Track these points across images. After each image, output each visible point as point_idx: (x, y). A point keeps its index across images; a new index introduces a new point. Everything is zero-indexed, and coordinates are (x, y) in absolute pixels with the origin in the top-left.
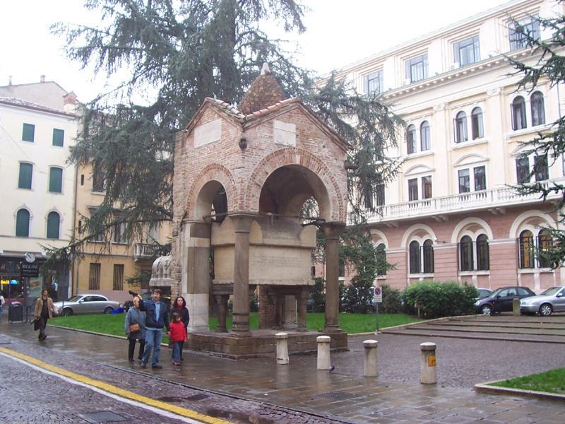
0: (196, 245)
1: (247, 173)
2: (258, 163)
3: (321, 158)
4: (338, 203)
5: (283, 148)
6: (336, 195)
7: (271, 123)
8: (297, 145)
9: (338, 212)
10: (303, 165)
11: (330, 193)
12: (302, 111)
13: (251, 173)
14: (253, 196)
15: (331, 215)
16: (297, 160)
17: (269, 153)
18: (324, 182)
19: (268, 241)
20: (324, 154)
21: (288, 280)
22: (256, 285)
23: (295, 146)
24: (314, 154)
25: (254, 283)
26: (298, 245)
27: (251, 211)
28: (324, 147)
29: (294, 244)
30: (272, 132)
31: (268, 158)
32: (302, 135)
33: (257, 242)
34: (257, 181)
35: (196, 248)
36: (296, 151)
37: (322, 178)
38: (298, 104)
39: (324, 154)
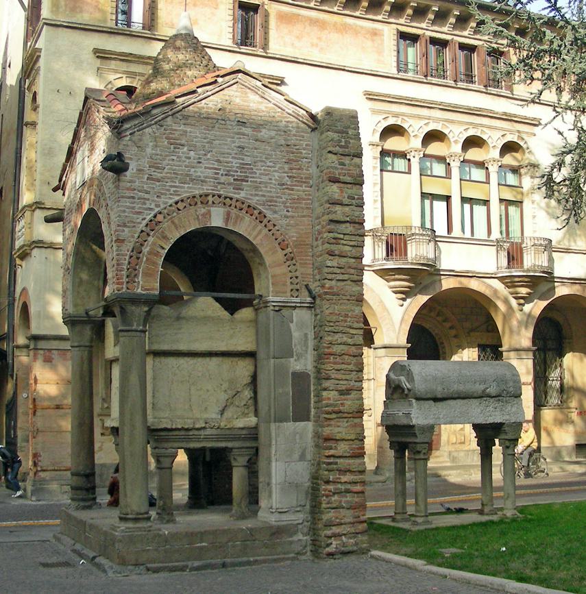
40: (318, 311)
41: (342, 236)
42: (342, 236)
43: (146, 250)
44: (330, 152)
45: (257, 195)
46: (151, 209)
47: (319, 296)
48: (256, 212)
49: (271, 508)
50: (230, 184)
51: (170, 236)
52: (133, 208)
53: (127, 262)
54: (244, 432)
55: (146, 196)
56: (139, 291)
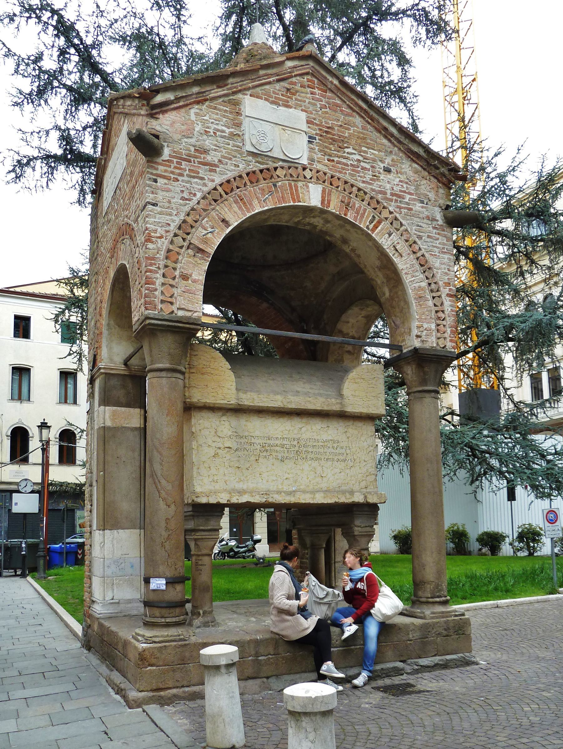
0: (109, 423)
1: (165, 219)
2: (199, 195)
3: (380, 197)
4: (430, 303)
5: (271, 165)
6: (424, 284)
7: (237, 103)
8: (311, 160)
9: (433, 326)
10: (332, 209)
11: (407, 279)
12: (323, 83)
13: (178, 220)
14: (185, 277)
15: (415, 332)
16: (313, 196)
17: (230, 175)
18: (391, 252)
19: (250, 399)
20: (388, 186)
21: (313, 492)
22: (215, 509)
23: (304, 161)
24: (362, 185)
25: (213, 501)
27: (180, 313)
28: (388, 170)
30: (238, 125)
31: (228, 186)
32: (325, 138)
33: (220, 401)
34: (196, 237)
35: (109, 428)
36: (308, 174)
37: (386, 242)
38: (311, 63)
39: (388, 186)
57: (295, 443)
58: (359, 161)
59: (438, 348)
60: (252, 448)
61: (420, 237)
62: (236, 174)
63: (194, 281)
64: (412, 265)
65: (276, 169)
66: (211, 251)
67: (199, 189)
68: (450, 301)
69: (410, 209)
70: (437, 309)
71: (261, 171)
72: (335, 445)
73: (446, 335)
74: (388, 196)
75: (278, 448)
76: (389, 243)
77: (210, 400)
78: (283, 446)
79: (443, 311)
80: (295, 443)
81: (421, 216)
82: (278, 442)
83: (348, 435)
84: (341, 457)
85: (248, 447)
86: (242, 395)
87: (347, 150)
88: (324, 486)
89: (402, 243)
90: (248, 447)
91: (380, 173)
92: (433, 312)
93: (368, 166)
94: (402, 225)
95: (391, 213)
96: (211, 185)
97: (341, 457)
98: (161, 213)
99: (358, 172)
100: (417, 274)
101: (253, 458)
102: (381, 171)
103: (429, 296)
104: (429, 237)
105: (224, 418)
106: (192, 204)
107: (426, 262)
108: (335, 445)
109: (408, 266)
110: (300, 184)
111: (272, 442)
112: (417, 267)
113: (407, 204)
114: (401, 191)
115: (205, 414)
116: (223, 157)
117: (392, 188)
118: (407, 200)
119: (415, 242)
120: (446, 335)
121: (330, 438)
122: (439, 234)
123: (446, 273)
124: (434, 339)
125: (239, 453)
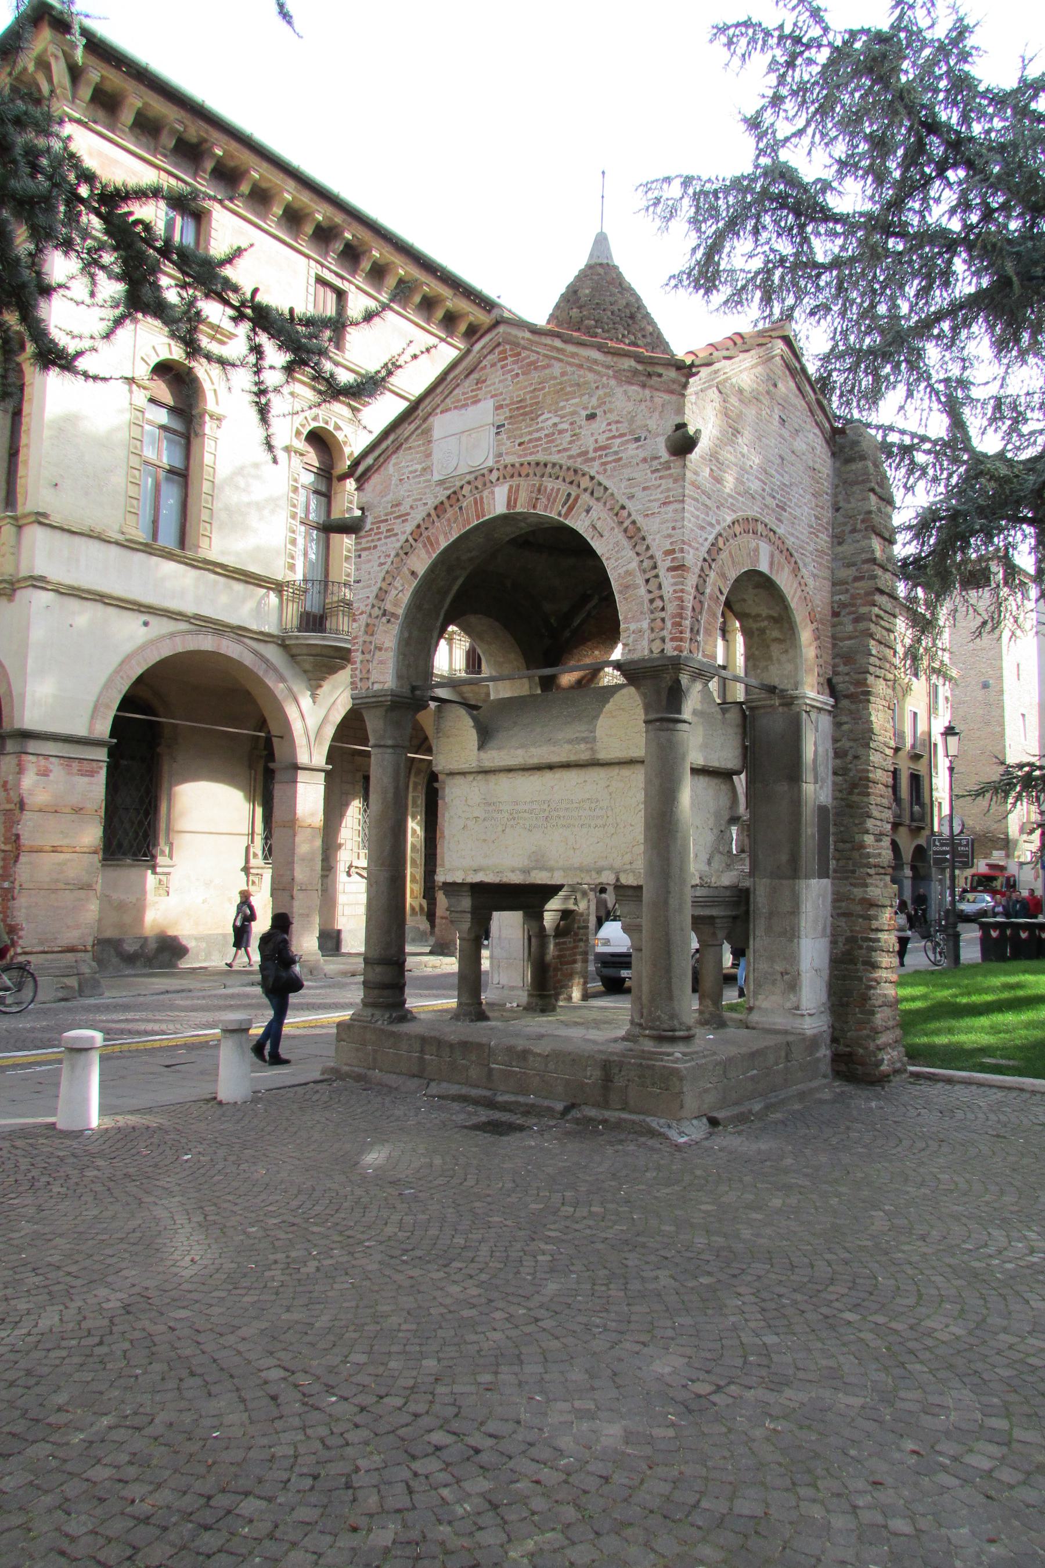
2: (393, 554)
4: (642, 591)
6: (634, 565)
26: (585, 756)
27: (376, 687)
28: (592, 417)
29: (573, 758)
33: (464, 767)
40: (844, 719)
41: (882, 613)
42: (882, 613)
43: (708, 591)
44: (872, 490)
45: (792, 535)
46: (712, 525)
47: (846, 697)
48: (793, 560)
49: (797, 1008)
50: (773, 510)
51: (728, 574)
52: (697, 518)
53: (690, 605)
54: (728, 893)
55: (708, 502)
56: (700, 657)
57: (545, 806)
58: (555, 425)
59: (655, 655)
60: (500, 816)
61: (631, 497)
62: (424, 514)
63: (386, 650)
64: (617, 543)
65: (462, 487)
66: (400, 611)
67: (393, 545)
68: (673, 577)
69: (620, 459)
70: (651, 596)
71: (449, 497)
72: (593, 805)
73: (665, 633)
74: (591, 455)
75: (526, 815)
76: (587, 523)
77: (455, 766)
78: (531, 812)
79: (661, 598)
80: (545, 806)
81: (635, 461)
82: (526, 807)
83: (611, 789)
84: (600, 822)
85: (495, 815)
86: (483, 755)
87: (540, 419)
88: (576, 861)
89: (604, 515)
90: (495, 815)
91: (580, 427)
92: (646, 602)
93: (565, 426)
94: (606, 489)
95: (592, 478)
96: (403, 538)
97: (600, 822)
98: (364, 588)
99: (552, 441)
100: (623, 553)
101: (500, 829)
102: (584, 423)
103: (640, 580)
104: (644, 489)
105: (475, 783)
106: (386, 567)
107: (639, 530)
108: (593, 805)
109: (611, 546)
110: (485, 493)
111: (519, 807)
112: (625, 542)
113: (616, 453)
114: (608, 439)
115: (459, 780)
116: (416, 500)
117: (596, 441)
118: (615, 449)
119: (623, 507)
120: (665, 633)
121: (587, 796)
122: (661, 478)
123: (670, 536)
124: (645, 643)
125: (486, 823)
